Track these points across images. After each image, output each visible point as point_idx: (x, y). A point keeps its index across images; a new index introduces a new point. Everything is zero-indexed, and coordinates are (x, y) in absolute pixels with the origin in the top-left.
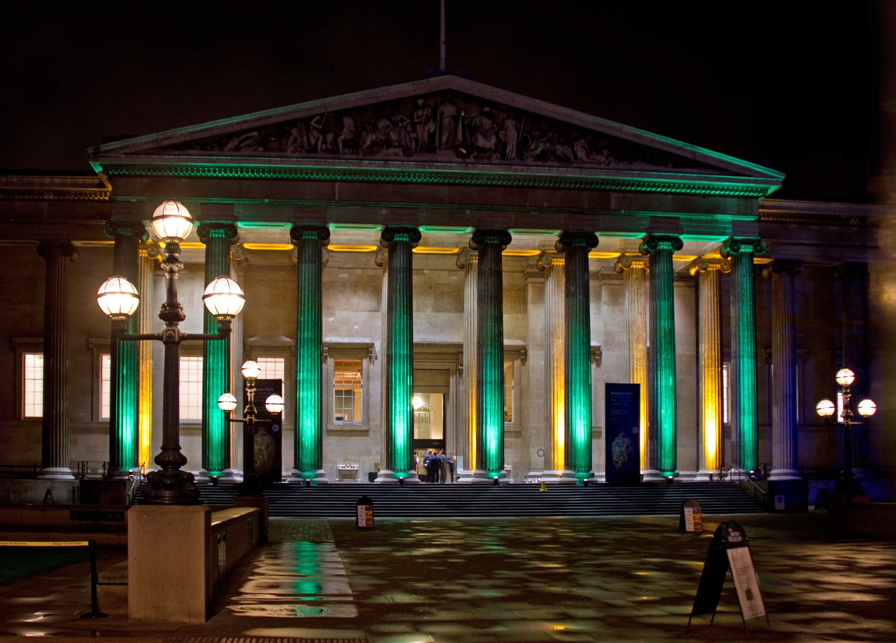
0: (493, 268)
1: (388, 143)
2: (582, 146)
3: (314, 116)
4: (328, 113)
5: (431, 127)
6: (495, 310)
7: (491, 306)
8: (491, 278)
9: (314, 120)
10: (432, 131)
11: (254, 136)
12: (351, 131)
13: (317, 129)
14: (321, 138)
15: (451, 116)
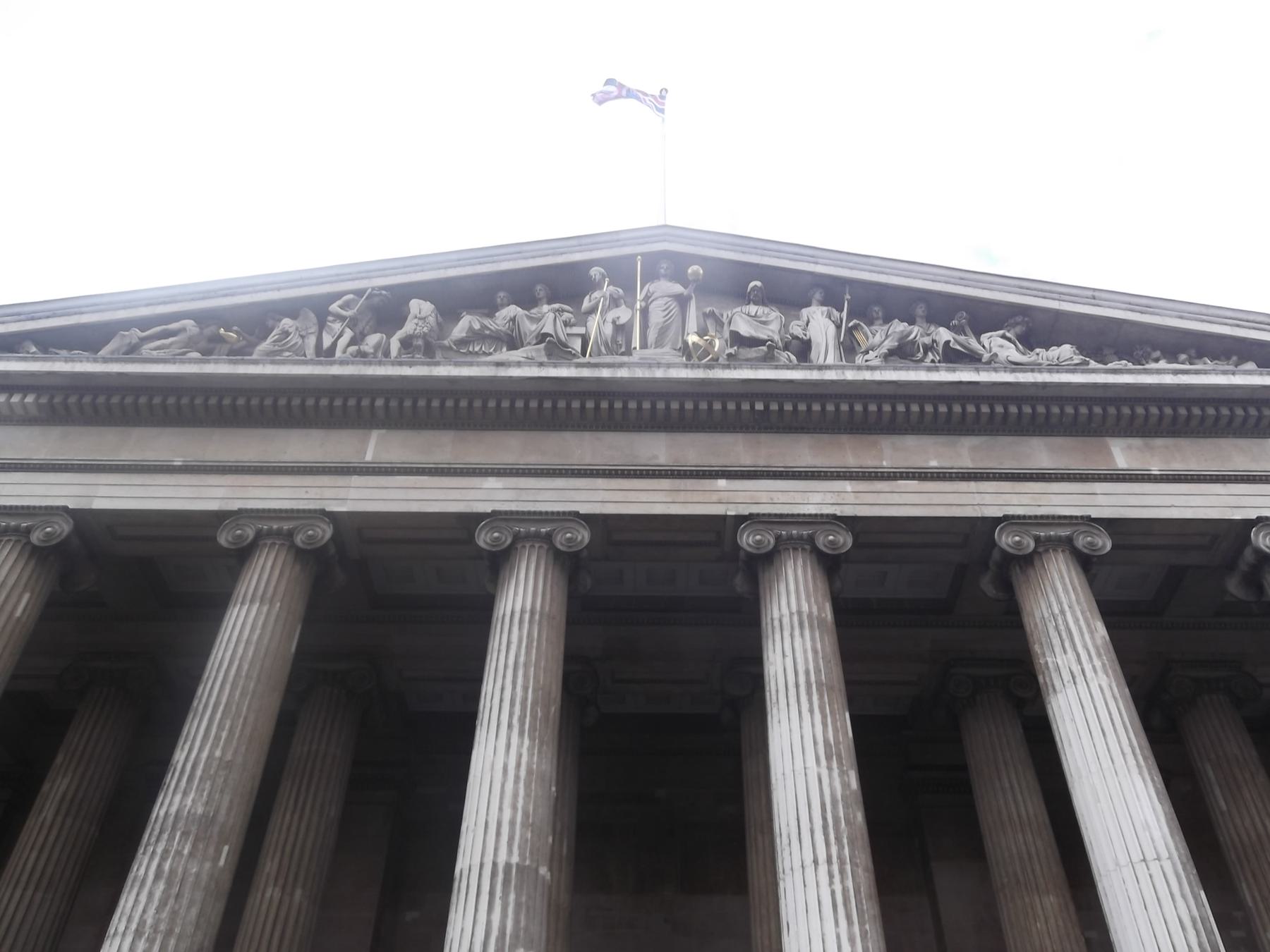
0: (805, 608)
1: (513, 341)
2: (1003, 337)
3: (339, 295)
4: (373, 289)
5: (623, 314)
6: (824, 724)
7: (811, 711)
8: (802, 635)
9: (339, 302)
10: (623, 320)
11: (183, 330)
12: (424, 319)
13: (342, 318)
14: (348, 334)
15: (669, 296)
